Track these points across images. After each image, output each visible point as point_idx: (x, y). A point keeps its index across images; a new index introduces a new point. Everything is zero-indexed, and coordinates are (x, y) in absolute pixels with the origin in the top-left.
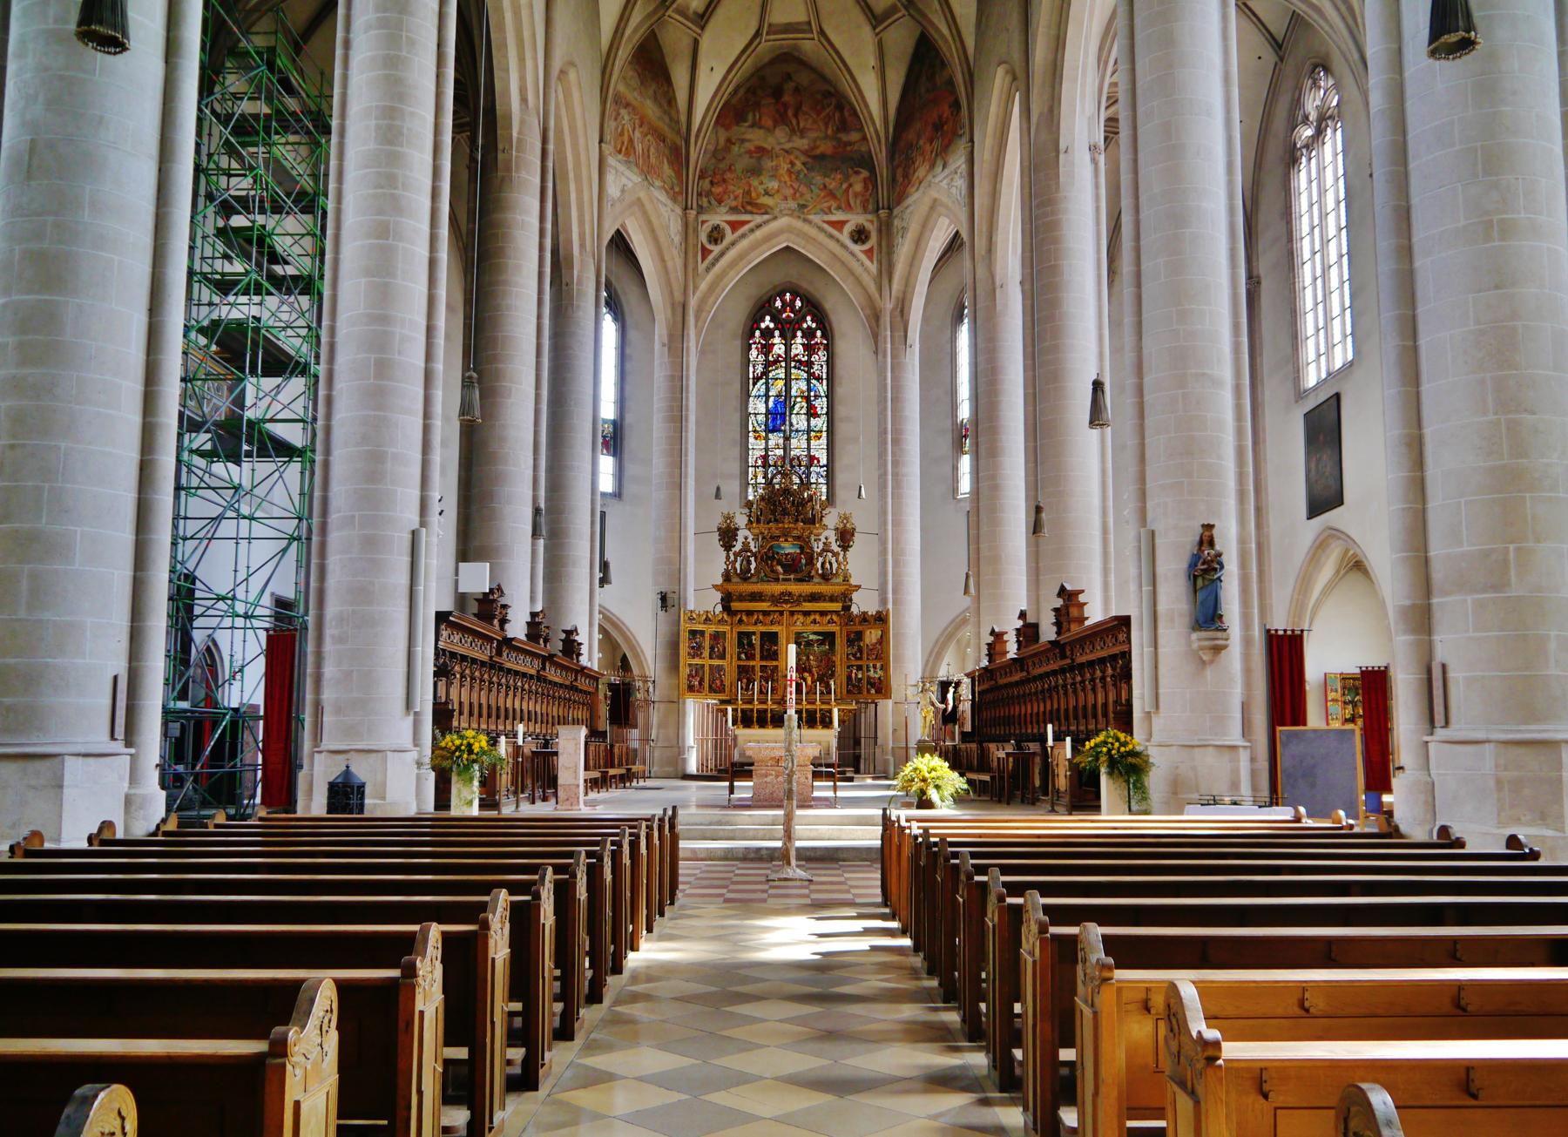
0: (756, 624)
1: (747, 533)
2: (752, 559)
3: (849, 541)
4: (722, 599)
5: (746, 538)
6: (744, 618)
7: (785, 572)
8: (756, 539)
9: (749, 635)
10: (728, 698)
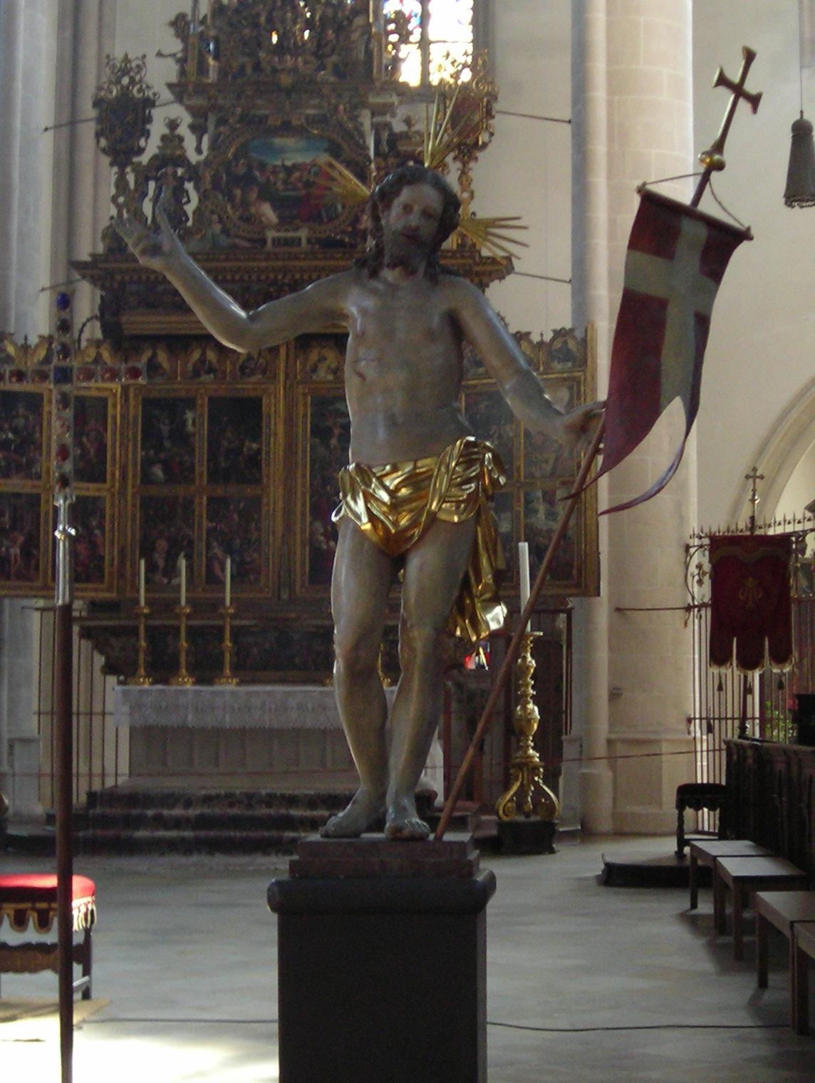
0: (196, 373)
1: (179, 112)
2: (189, 186)
3: (476, 130)
4: (103, 307)
5: (173, 125)
6: (162, 357)
7: (284, 221)
8: (198, 129)
9: (174, 407)
10: (113, 595)
